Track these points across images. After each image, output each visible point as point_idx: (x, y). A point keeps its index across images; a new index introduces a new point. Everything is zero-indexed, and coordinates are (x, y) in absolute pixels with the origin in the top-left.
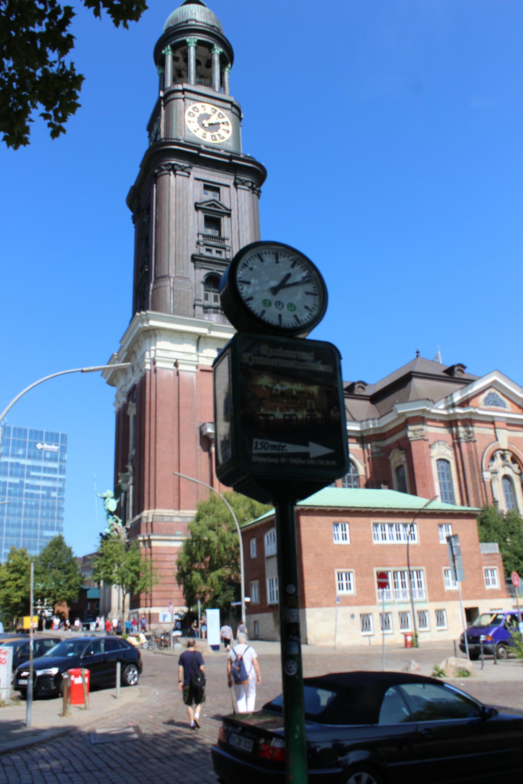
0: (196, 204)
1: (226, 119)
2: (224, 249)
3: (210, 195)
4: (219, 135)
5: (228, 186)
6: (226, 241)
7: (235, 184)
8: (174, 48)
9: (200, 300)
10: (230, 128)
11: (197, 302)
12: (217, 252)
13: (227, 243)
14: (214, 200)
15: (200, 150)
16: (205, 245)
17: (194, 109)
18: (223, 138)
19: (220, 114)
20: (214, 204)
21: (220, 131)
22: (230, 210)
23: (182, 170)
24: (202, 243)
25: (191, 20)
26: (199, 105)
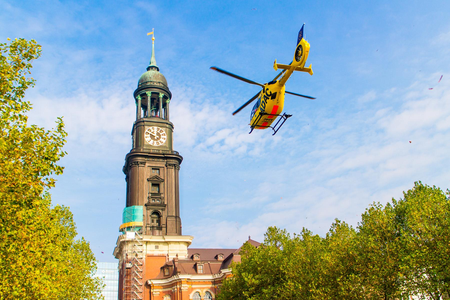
0: (148, 179)
1: (164, 132)
2: (161, 198)
3: (156, 173)
4: (160, 141)
5: (164, 167)
6: (162, 195)
7: (166, 166)
8: (141, 96)
9: (149, 224)
10: (165, 137)
11: (147, 226)
12: (157, 200)
13: (162, 195)
14: (156, 176)
15: (149, 153)
16: (151, 198)
17: (148, 130)
18: (162, 143)
19: (161, 130)
20: (156, 177)
21: (161, 139)
22: (164, 180)
23: (142, 164)
24: (150, 198)
25: (149, 82)
26: (151, 128)
